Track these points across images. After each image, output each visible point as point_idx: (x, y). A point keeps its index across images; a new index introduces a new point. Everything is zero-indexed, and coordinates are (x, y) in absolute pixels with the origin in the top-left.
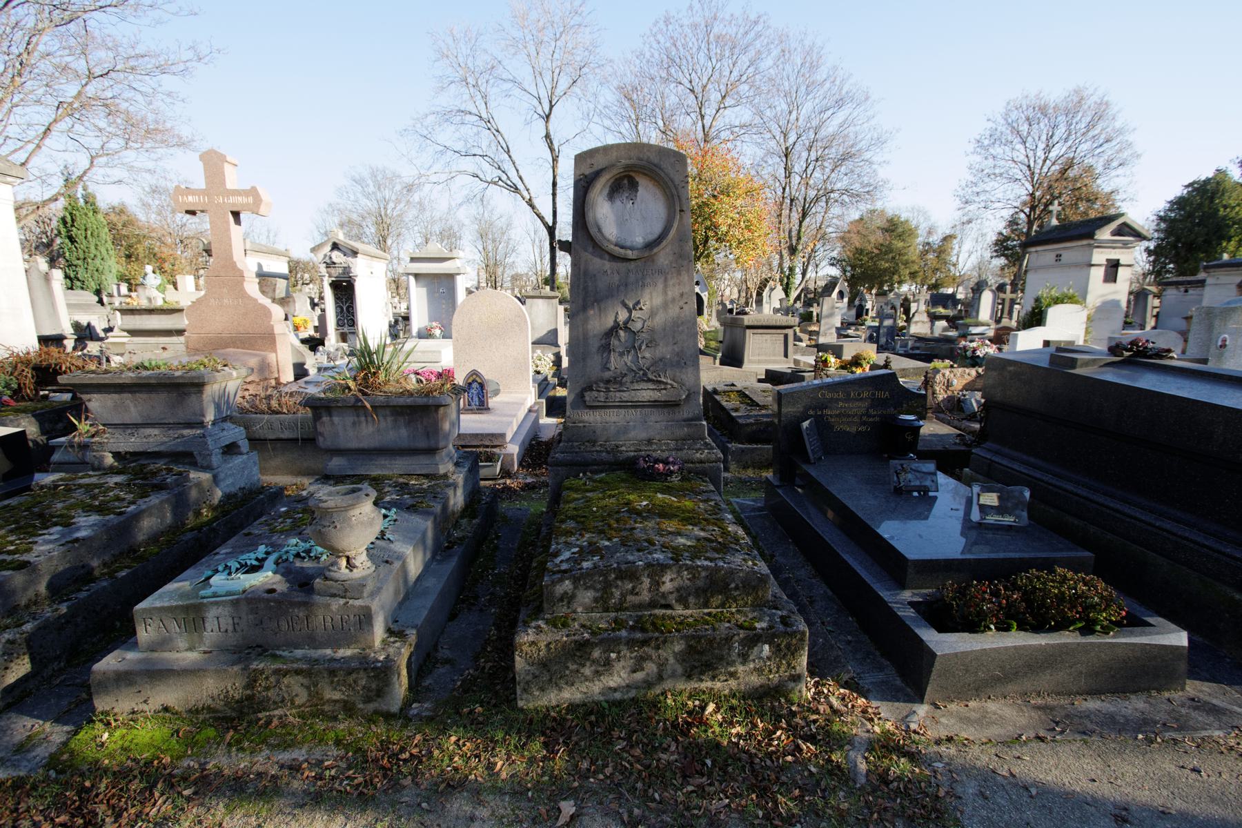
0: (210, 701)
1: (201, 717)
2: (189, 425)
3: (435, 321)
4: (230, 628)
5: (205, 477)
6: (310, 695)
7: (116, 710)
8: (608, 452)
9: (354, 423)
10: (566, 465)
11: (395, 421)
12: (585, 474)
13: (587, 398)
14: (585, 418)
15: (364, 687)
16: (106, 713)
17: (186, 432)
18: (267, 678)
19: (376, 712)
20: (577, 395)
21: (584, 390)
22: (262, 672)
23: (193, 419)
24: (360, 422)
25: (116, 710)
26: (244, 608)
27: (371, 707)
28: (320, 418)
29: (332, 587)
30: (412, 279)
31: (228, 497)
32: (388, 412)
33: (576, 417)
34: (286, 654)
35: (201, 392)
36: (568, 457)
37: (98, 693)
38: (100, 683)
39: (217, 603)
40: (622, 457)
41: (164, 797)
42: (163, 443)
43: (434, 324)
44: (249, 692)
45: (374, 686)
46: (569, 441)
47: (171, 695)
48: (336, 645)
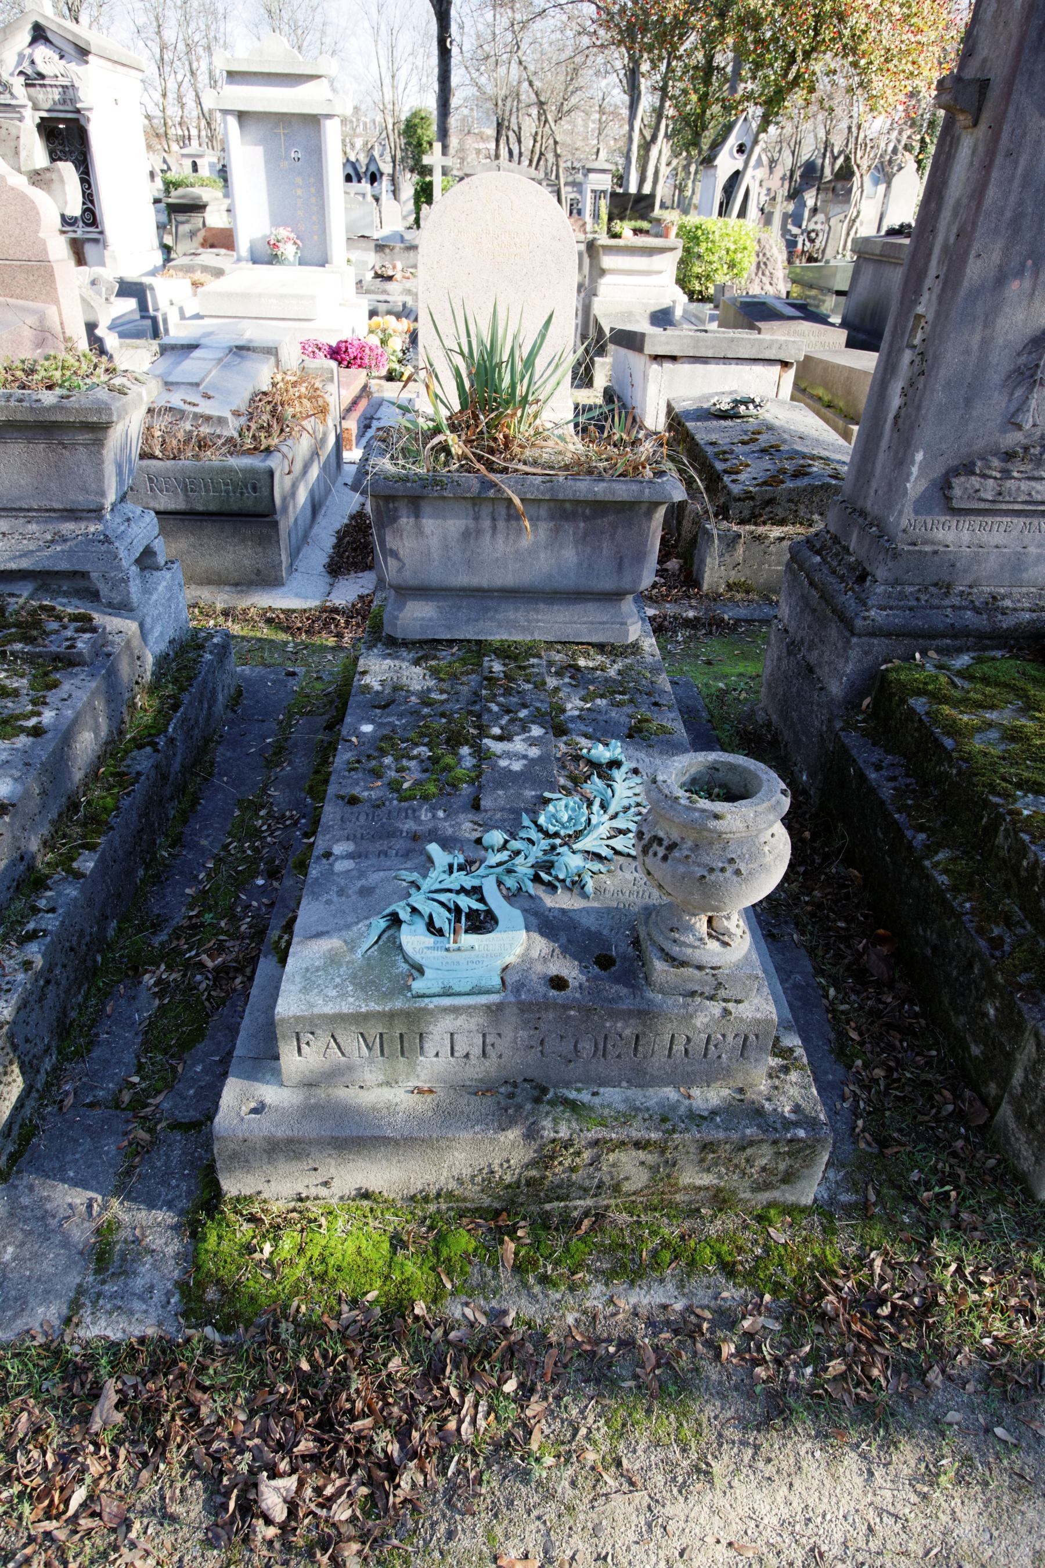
0: (452, 1185)
1: (432, 1208)
2: (72, 514)
3: (285, 225)
4: (477, 1051)
5: (132, 627)
6: (652, 1179)
7: (263, 1196)
8: (977, 611)
9: (466, 535)
10: (888, 635)
11: (557, 531)
12: (924, 654)
13: (957, 492)
14: (940, 534)
15: (764, 1169)
16: (249, 1199)
17: (68, 527)
18: (578, 1154)
19: (770, 1205)
20: (933, 483)
21: (955, 471)
22: (567, 1144)
23: (80, 499)
24: (479, 532)
25: (263, 1196)
26: (511, 1017)
27: (765, 1197)
28: (395, 519)
29: (691, 979)
30: (232, 122)
31: (162, 661)
32: (543, 512)
33: (920, 531)
34: (585, 1097)
35: (99, 443)
36: (898, 619)
37: (229, 1170)
38: (234, 1156)
39: (455, 1010)
40: (1007, 622)
41: (470, 1398)
42: (25, 554)
43: (283, 232)
44: (534, 1173)
45: (782, 1166)
46: (896, 582)
47: (383, 1175)
48: (684, 1079)
